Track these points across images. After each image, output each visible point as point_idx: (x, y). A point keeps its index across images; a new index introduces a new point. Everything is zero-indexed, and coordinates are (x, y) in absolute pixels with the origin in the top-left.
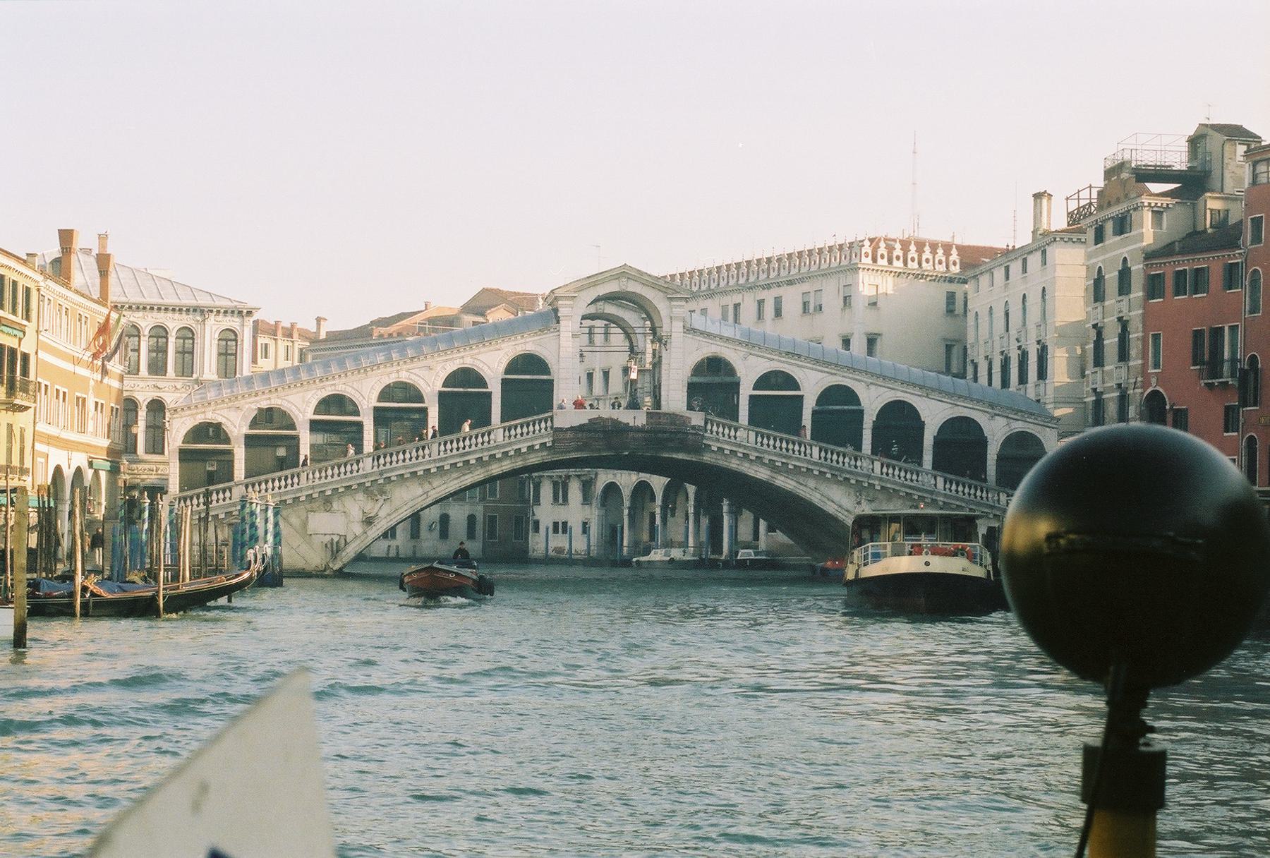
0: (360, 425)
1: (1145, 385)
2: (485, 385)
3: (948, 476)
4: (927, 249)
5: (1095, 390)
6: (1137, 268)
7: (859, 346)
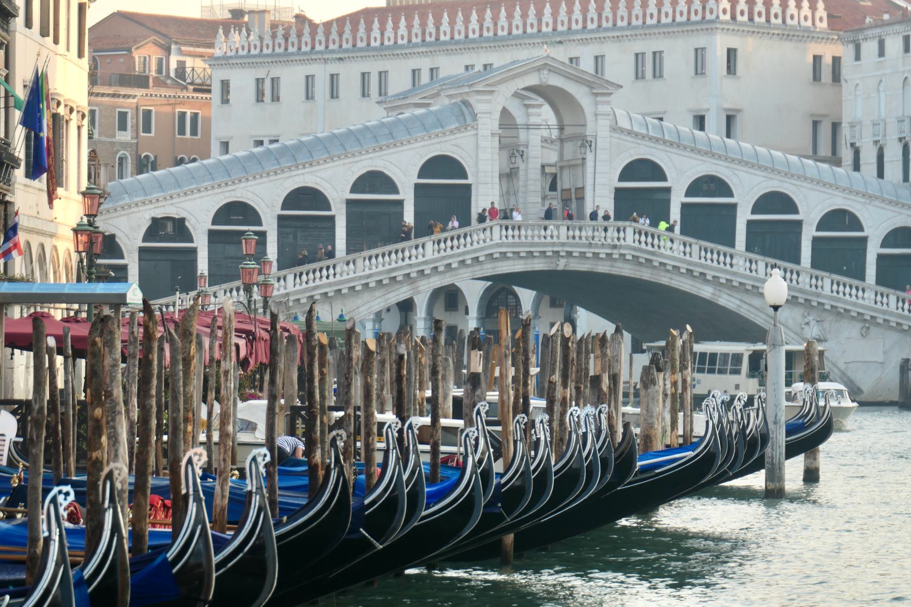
2: (397, 192)
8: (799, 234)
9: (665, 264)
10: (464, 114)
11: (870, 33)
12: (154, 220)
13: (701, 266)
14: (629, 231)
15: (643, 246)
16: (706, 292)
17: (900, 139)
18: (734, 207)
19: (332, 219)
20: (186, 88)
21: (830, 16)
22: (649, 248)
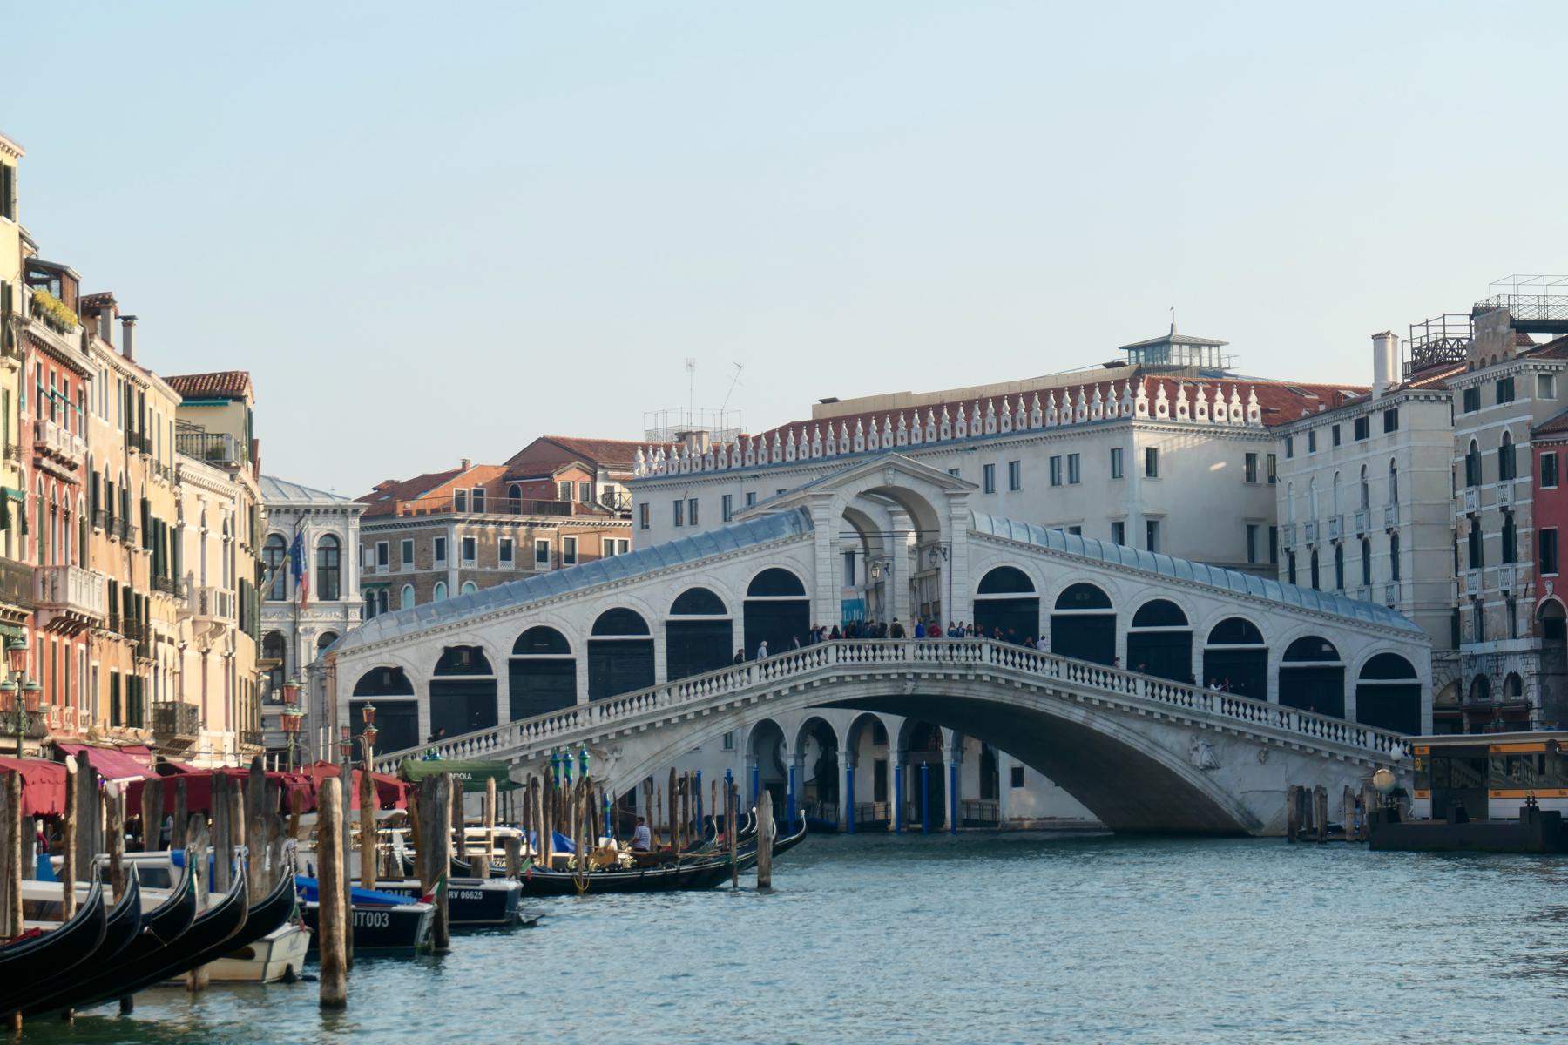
0: (572, 662)
1: (1539, 592)
3: (1304, 713)
4: (1219, 396)
5: (1473, 597)
6: (1523, 446)
7: (1135, 532)
8: (1189, 646)
9: (1028, 686)
10: (803, 520)
11: (1299, 425)
12: (447, 650)
13: (1070, 686)
14: (986, 649)
15: (1002, 665)
16: (1078, 715)
17: (1333, 542)
18: (1112, 618)
19: (650, 643)
20: (611, 515)
21: (1263, 411)
22: (1010, 667)
